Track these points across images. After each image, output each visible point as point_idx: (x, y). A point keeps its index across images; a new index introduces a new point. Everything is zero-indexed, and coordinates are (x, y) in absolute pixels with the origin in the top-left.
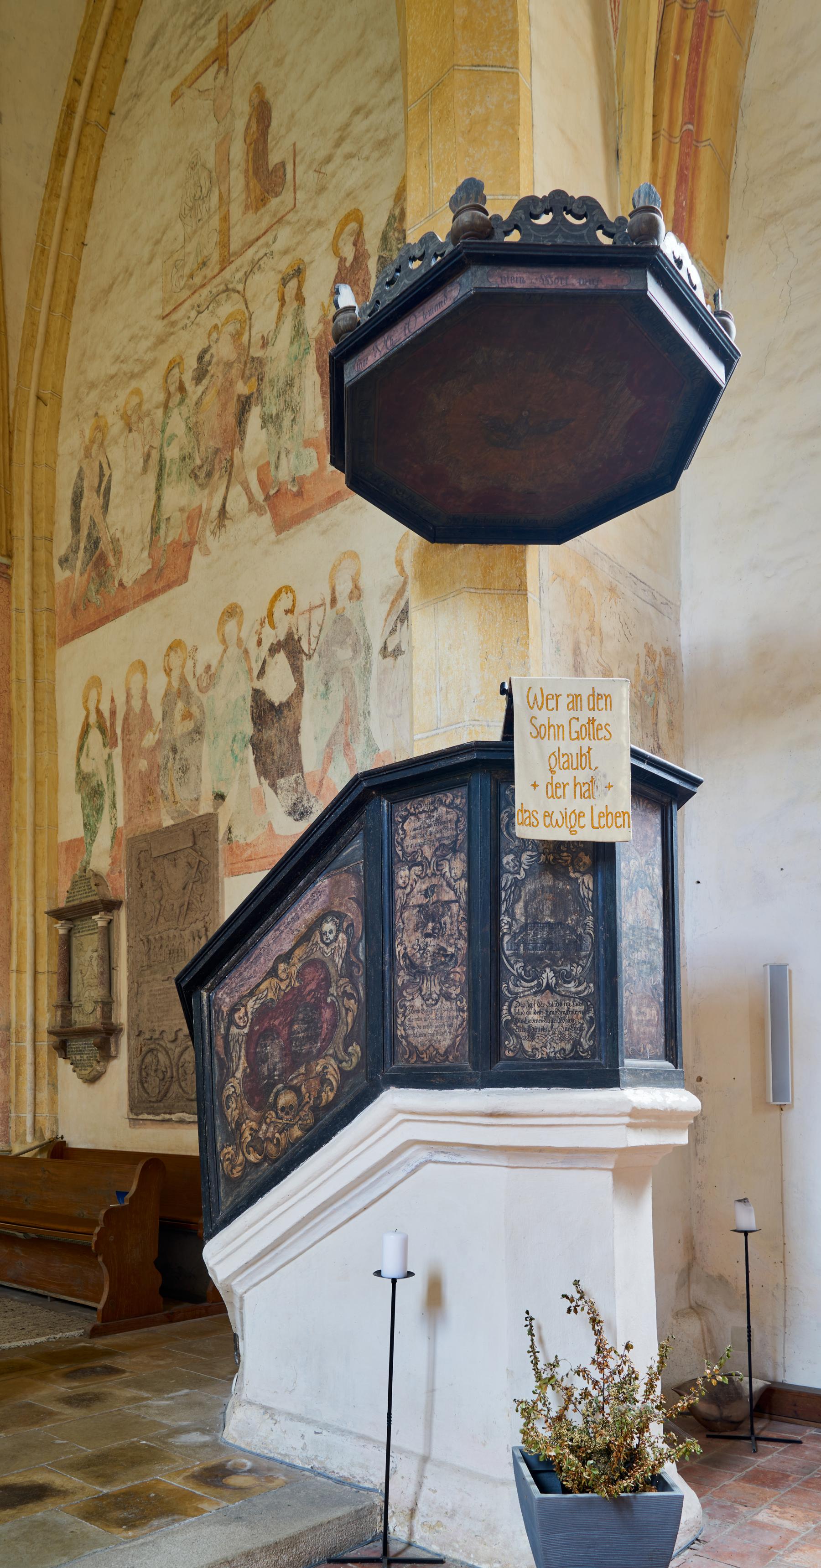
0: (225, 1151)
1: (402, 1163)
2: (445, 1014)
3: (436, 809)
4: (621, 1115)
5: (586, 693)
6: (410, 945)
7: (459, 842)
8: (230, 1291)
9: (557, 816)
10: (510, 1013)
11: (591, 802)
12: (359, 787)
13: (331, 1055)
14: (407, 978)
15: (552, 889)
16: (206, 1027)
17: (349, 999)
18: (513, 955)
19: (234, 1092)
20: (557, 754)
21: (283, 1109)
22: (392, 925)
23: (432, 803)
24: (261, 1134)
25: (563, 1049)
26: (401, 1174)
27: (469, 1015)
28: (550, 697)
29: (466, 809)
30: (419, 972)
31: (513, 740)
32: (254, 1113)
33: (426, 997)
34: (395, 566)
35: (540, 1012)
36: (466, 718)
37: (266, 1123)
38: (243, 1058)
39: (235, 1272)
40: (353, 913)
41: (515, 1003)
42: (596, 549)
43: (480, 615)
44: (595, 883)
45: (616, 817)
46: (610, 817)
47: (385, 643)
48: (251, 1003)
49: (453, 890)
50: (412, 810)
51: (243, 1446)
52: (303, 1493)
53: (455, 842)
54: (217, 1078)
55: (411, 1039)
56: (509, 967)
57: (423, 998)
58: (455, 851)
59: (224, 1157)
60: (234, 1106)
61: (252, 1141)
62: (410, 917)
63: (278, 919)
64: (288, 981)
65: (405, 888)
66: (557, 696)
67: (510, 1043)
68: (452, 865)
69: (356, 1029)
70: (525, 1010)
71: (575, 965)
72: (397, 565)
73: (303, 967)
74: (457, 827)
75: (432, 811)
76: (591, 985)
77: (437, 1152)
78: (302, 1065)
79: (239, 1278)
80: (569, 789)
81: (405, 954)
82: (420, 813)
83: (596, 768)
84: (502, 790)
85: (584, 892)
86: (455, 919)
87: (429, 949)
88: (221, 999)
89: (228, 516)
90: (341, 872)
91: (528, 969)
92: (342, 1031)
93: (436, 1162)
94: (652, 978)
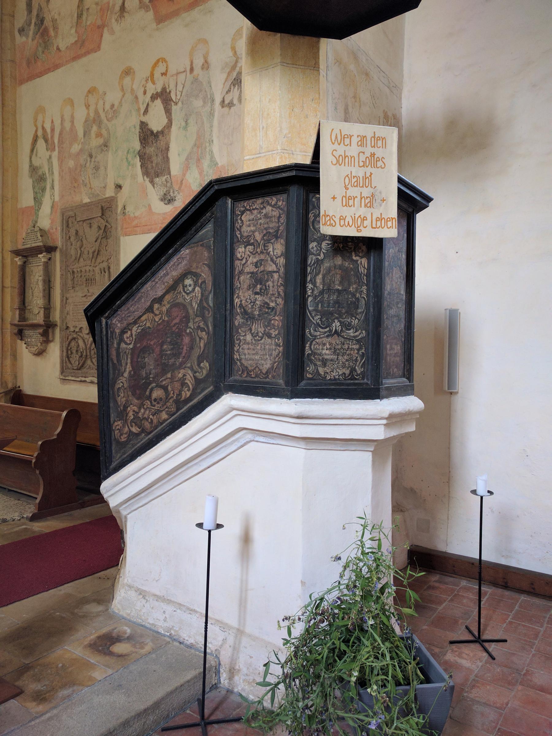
0: (116, 424)
1: (234, 441)
2: (267, 347)
3: (264, 207)
4: (382, 418)
5: (369, 135)
6: (244, 299)
7: (280, 231)
8: (118, 512)
10: (311, 349)
11: (372, 210)
12: (212, 189)
13: (188, 367)
14: (241, 321)
15: (341, 267)
16: (105, 342)
17: (202, 331)
18: (314, 310)
19: (123, 386)
20: (350, 176)
21: (155, 400)
22: (232, 284)
23: (262, 203)
24: (140, 415)
25: (344, 374)
26: (233, 448)
27: (284, 349)
28: (346, 136)
29: (286, 209)
30: (250, 317)
31: (319, 164)
32: (136, 401)
33: (255, 334)
34: (230, 50)
35: (330, 349)
36: (279, 148)
37: (144, 408)
38: (129, 364)
39: (121, 503)
40: (206, 274)
41: (314, 343)
42: (359, 47)
43: (290, 81)
44: (369, 263)
45: (387, 221)
46: (383, 221)
47: (224, 98)
48: (135, 329)
49: (275, 264)
50: (248, 207)
51: (125, 615)
52: (164, 658)
53: (277, 231)
54: (111, 376)
55: (243, 361)
56: (311, 318)
57: (252, 335)
58: (277, 237)
59: (116, 428)
60: (122, 395)
61: (134, 418)
62: (244, 281)
63: (153, 274)
64: (160, 316)
65: (242, 260)
66: (351, 136)
67: (310, 368)
68: (275, 247)
69: (206, 351)
70: (321, 347)
71: (354, 318)
72: (232, 50)
73: (171, 308)
74: (279, 221)
75: (262, 209)
76: (364, 332)
77: (258, 435)
78: (169, 372)
79: (124, 506)
81: (241, 304)
82: (253, 209)
83: (375, 187)
84: (310, 197)
85: (361, 270)
86: (275, 284)
87: (257, 302)
88: (114, 324)
89: (126, 10)
90: (198, 246)
91: (323, 320)
92: (196, 352)
93: (257, 441)
94: (398, 325)
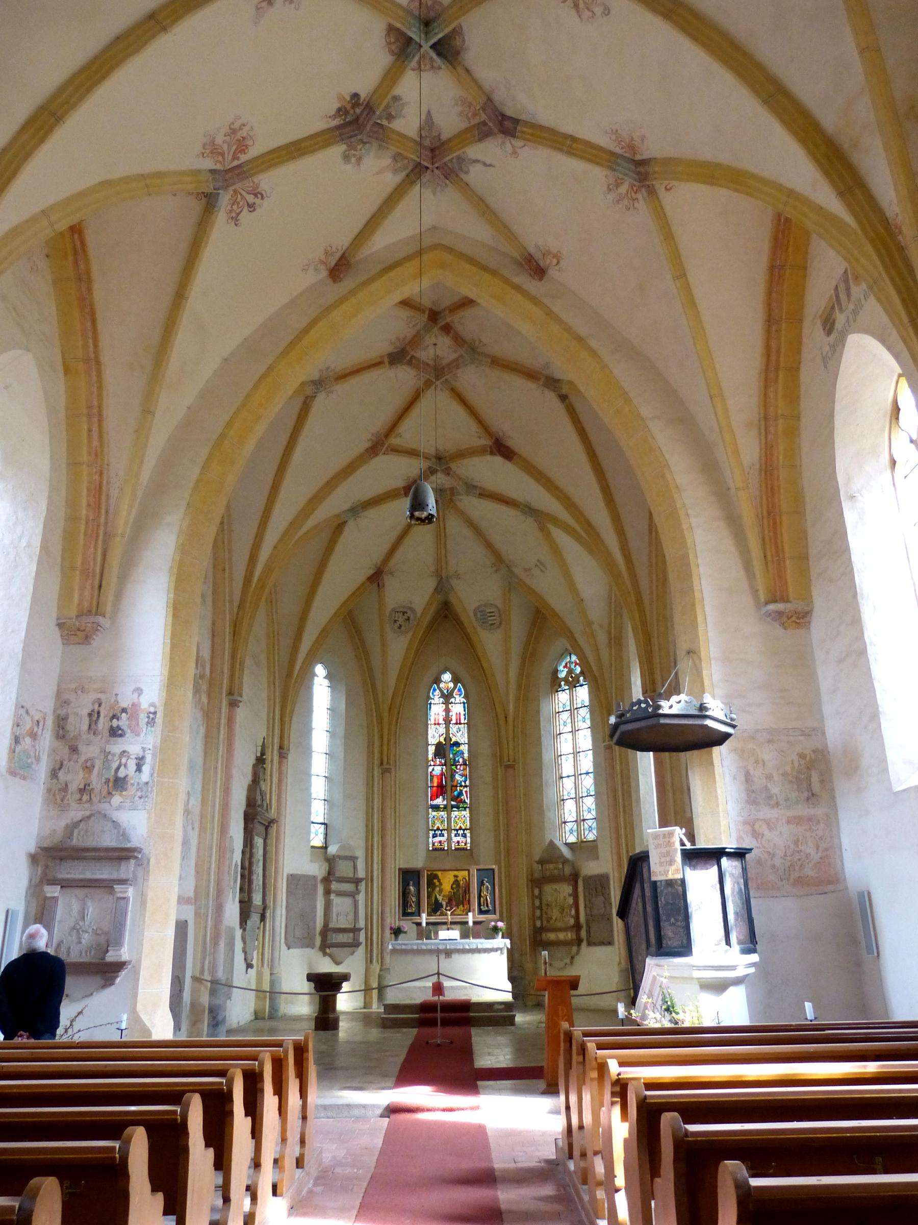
9: (662, 872)
67: (664, 942)
80: (665, 863)
